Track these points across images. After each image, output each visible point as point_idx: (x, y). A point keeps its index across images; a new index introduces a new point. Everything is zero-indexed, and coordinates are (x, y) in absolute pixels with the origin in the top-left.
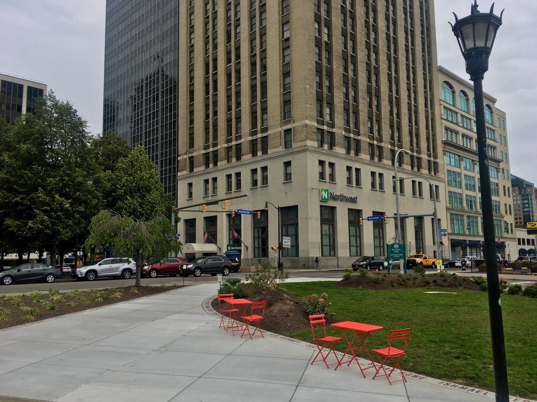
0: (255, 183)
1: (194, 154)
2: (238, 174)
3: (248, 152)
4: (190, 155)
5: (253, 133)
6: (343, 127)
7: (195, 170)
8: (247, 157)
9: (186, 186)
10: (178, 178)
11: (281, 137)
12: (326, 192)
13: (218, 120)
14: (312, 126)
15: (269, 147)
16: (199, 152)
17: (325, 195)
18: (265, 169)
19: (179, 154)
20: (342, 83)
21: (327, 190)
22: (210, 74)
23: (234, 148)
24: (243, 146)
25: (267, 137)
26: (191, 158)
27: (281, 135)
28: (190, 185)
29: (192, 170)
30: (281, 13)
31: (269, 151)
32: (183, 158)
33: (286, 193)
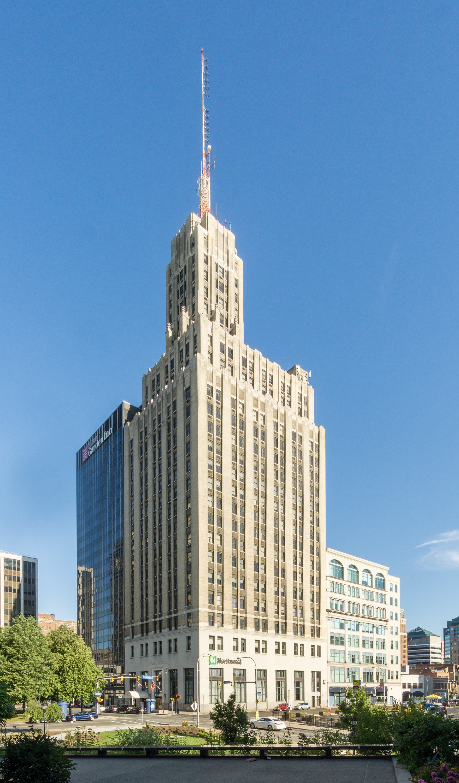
0: (170, 650)
1: (135, 625)
2: (161, 642)
3: (166, 627)
4: (132, 625)
5: (170, 613)
6: (231, 609)
7: (135, 637)
8: (166, 630)
9: (130, 648)
10: (125, 641)
11: (185, 618)
12: (215, 658)
13: (149, 601)
14: (204, 611)
15: (178, 625)
16: (137, 624)
17: (213, 661)
18: (176, 640)
19: (125, 623)
20: (231, 575)
21: (215, 657)
22: (144, 565)
23: (158, 622)
24: (163, 622)
25: (177, 617)
26: (133, 627)
27: (185, 617)
28: (132, 647)
29: (133, 637)
30: (186, 526)
31: (178, 628)
32: (128, 626)
33: (188, 659)
